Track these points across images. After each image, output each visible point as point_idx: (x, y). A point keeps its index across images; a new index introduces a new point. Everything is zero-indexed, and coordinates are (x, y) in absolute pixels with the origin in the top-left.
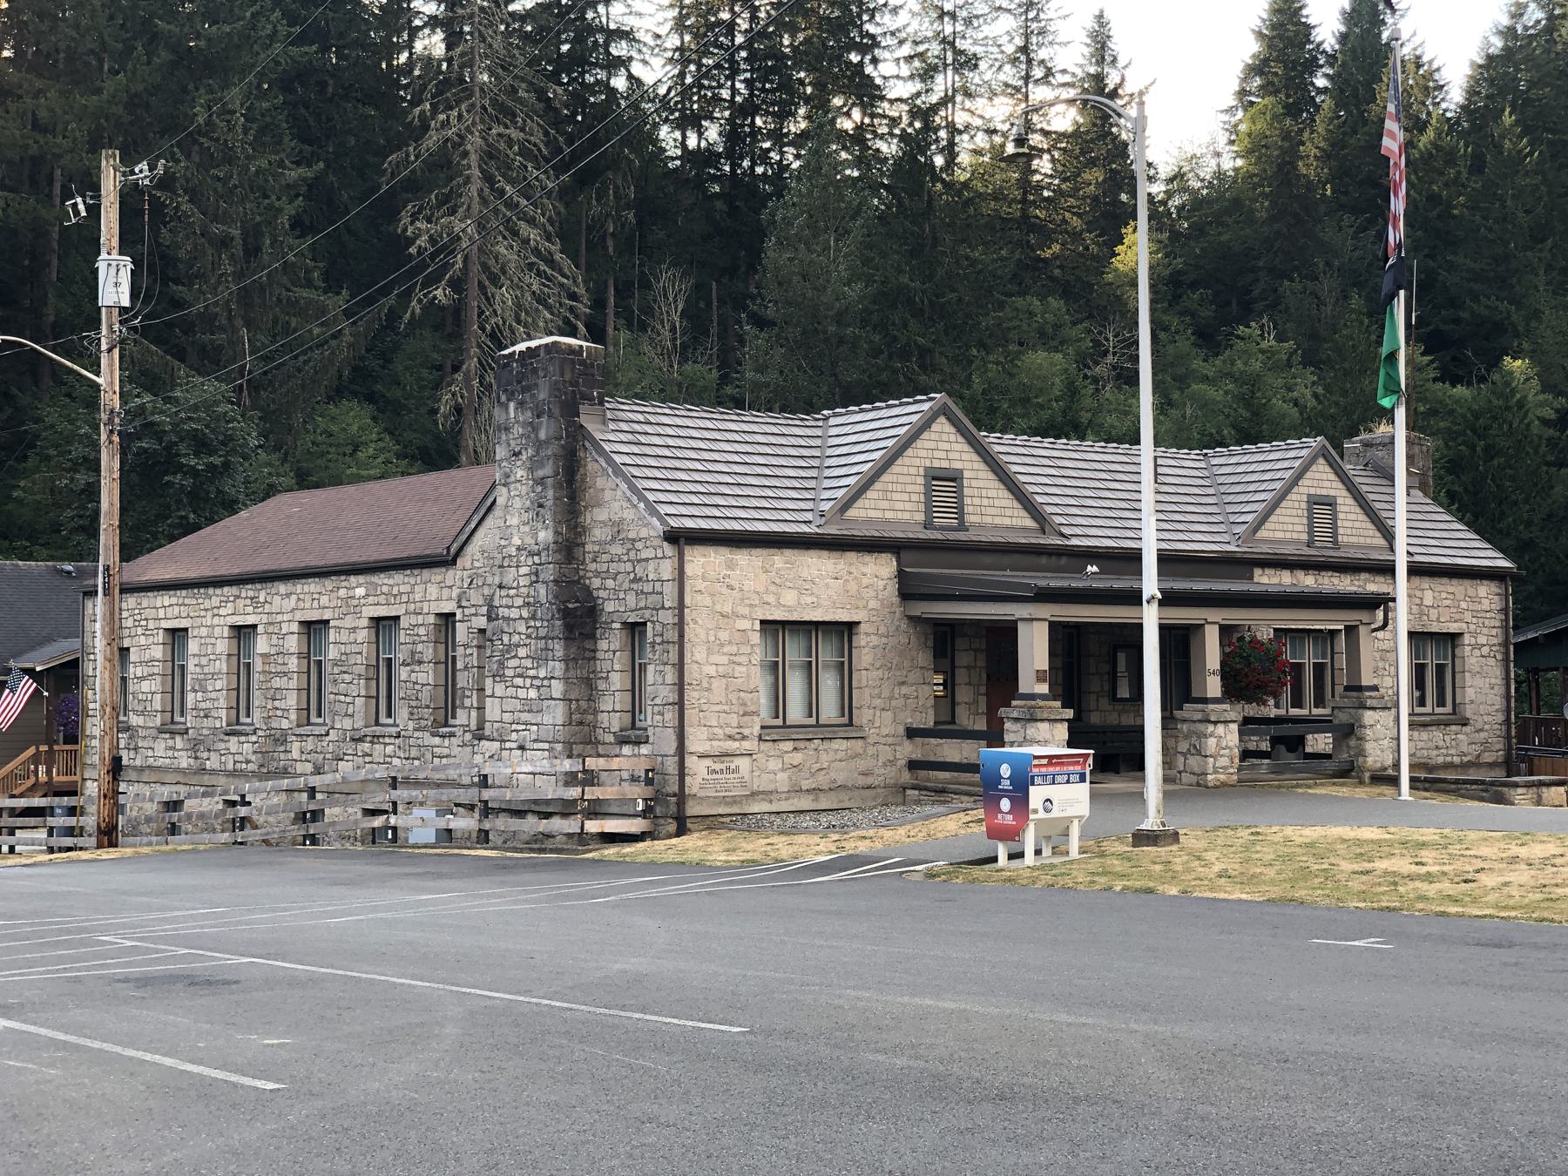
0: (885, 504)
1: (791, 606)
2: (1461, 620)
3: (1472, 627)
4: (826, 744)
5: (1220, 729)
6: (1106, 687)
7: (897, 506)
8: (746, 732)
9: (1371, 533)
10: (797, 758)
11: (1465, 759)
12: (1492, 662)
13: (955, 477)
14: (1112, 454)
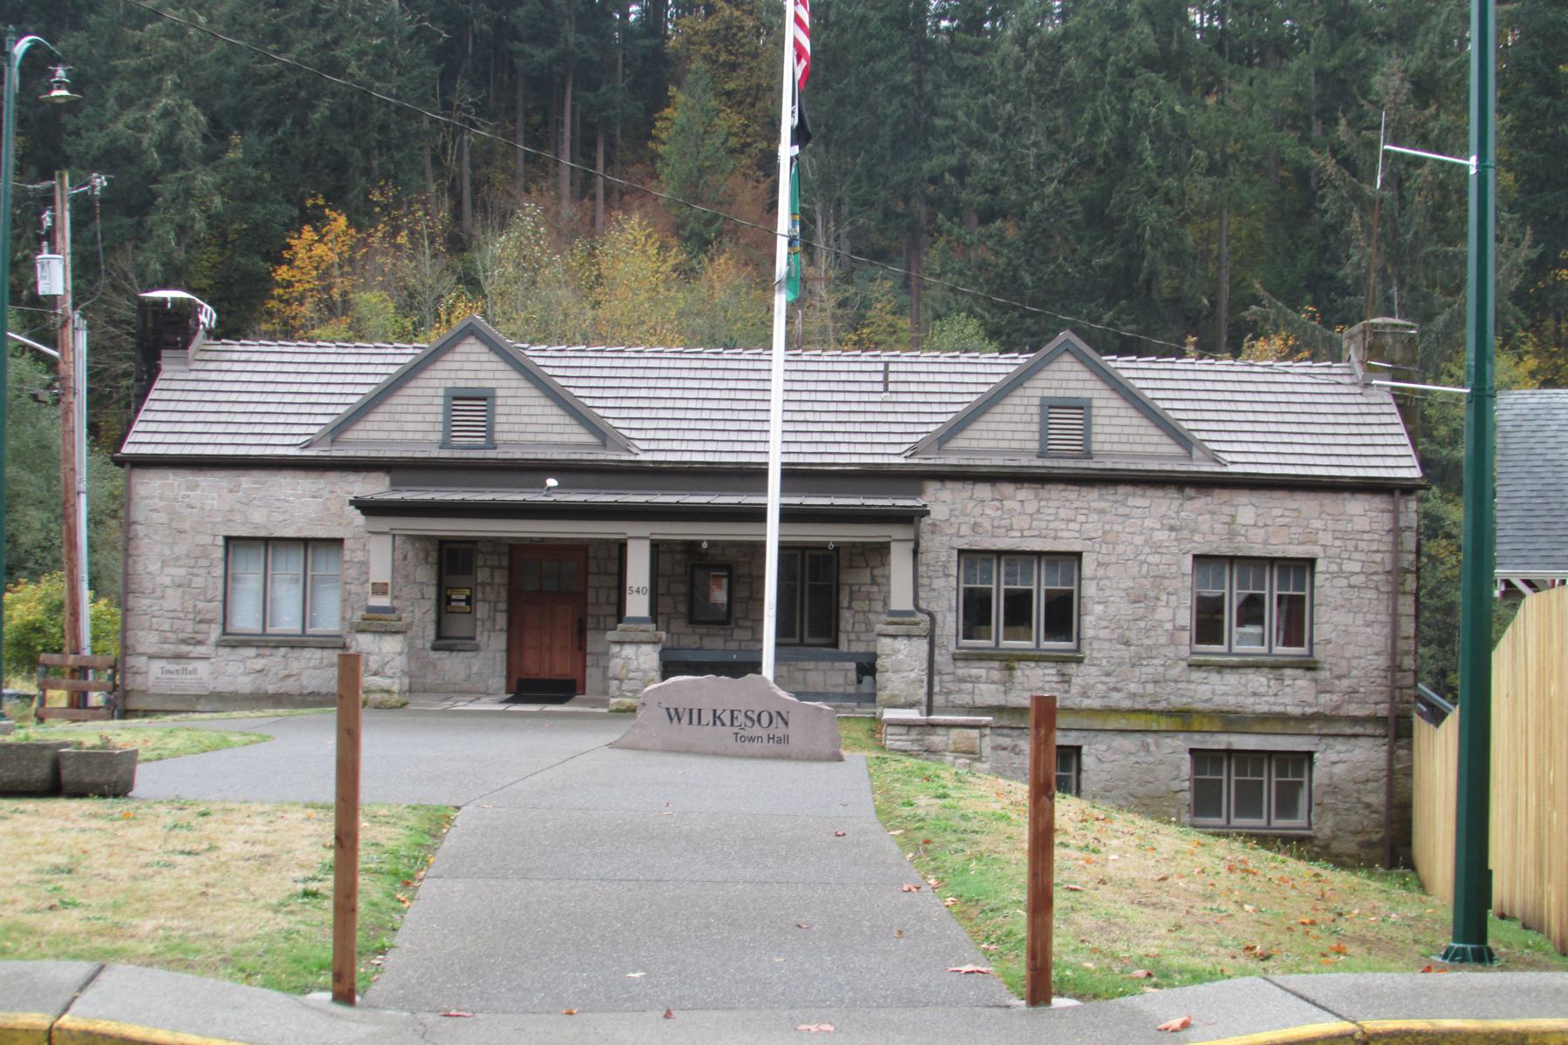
0: (393, 426)
1: (259, 521)
2: (1315, 542)
3: (1331, 552)
4: (296, 653)
5: (629, 651)
6: (682, 608)
7: (412, 427)
8: (200, 637)
9: (1156, 439)
10: (260, 664)
11: (1309, 710)
12: (1372, 594)
13: (484, 397)
14: (741, 359)
